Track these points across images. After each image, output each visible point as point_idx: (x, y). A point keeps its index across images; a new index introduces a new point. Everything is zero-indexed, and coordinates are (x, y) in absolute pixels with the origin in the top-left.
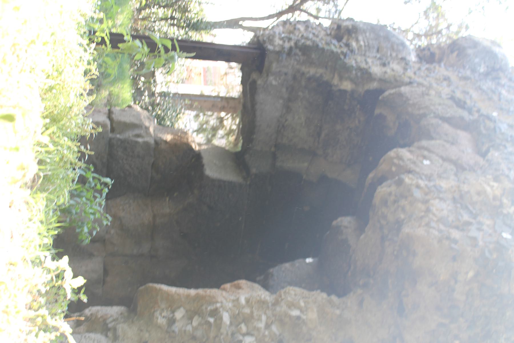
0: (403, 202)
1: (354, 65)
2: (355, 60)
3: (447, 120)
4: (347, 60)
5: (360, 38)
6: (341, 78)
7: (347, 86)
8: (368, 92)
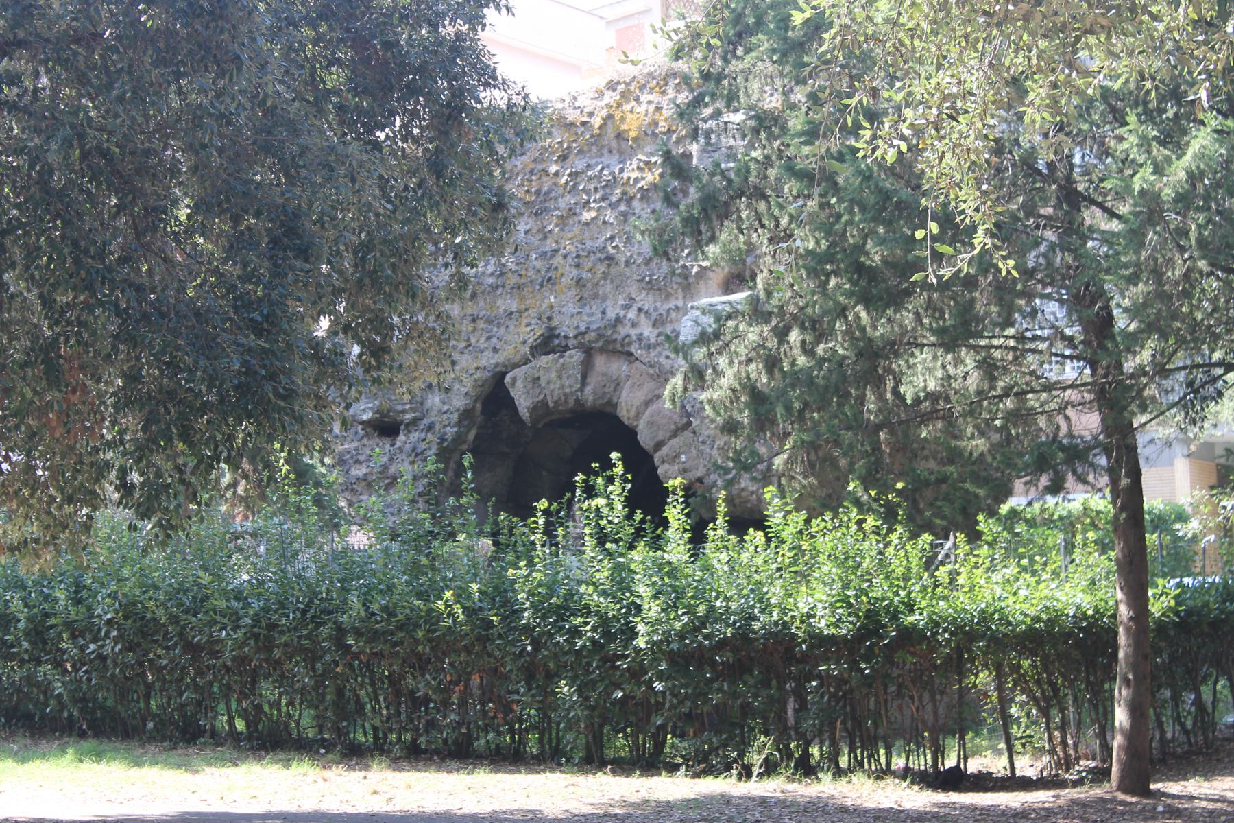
0: (737, 501)
1: (455, 429)
2: (445, 426)
3: (584, 377)
4: (449, 437)
5: (399, 408)
6: (465, 442)
7: (471, 435)
8: (483, 412)
